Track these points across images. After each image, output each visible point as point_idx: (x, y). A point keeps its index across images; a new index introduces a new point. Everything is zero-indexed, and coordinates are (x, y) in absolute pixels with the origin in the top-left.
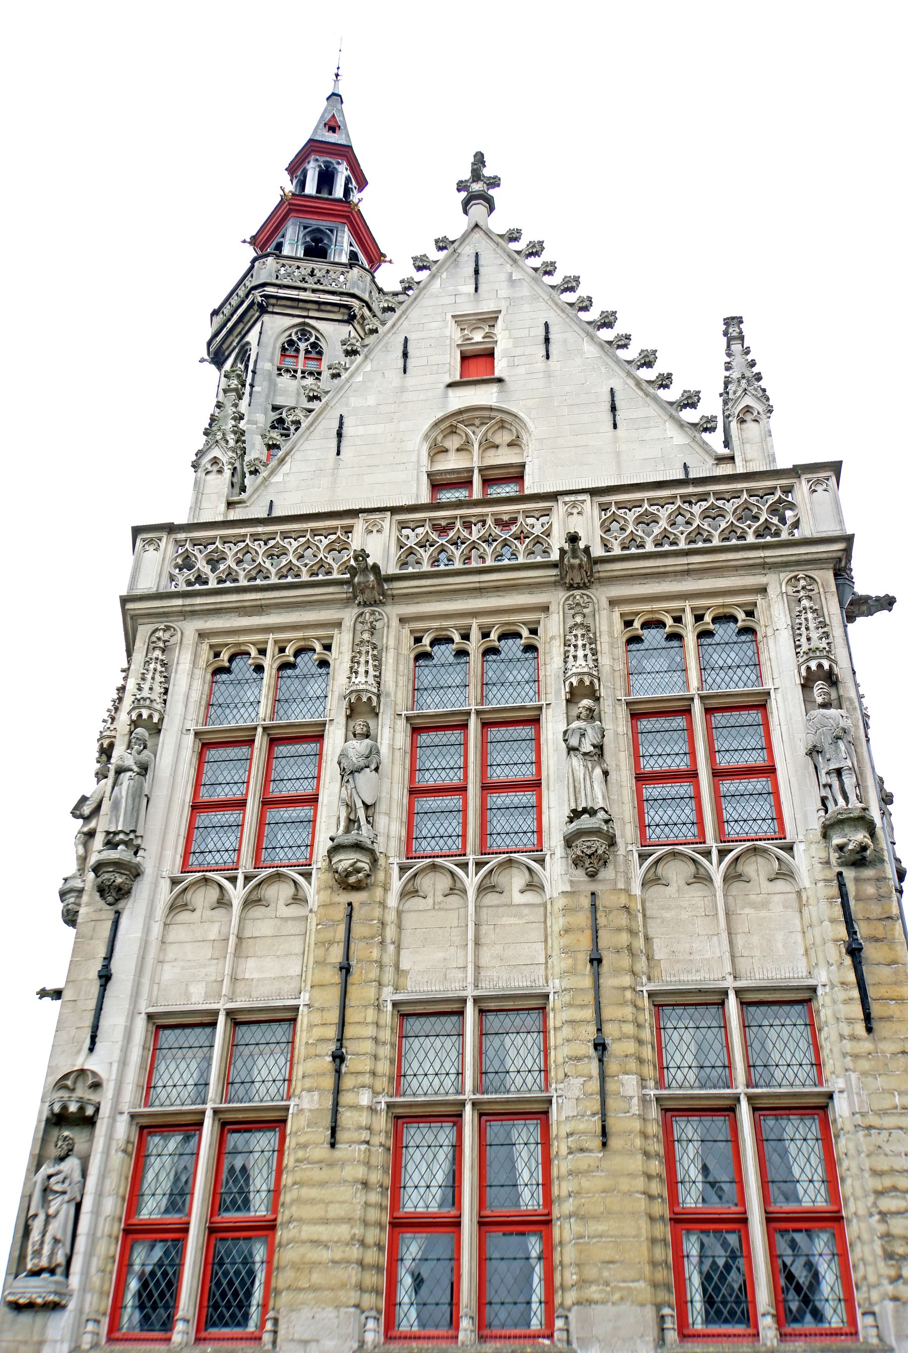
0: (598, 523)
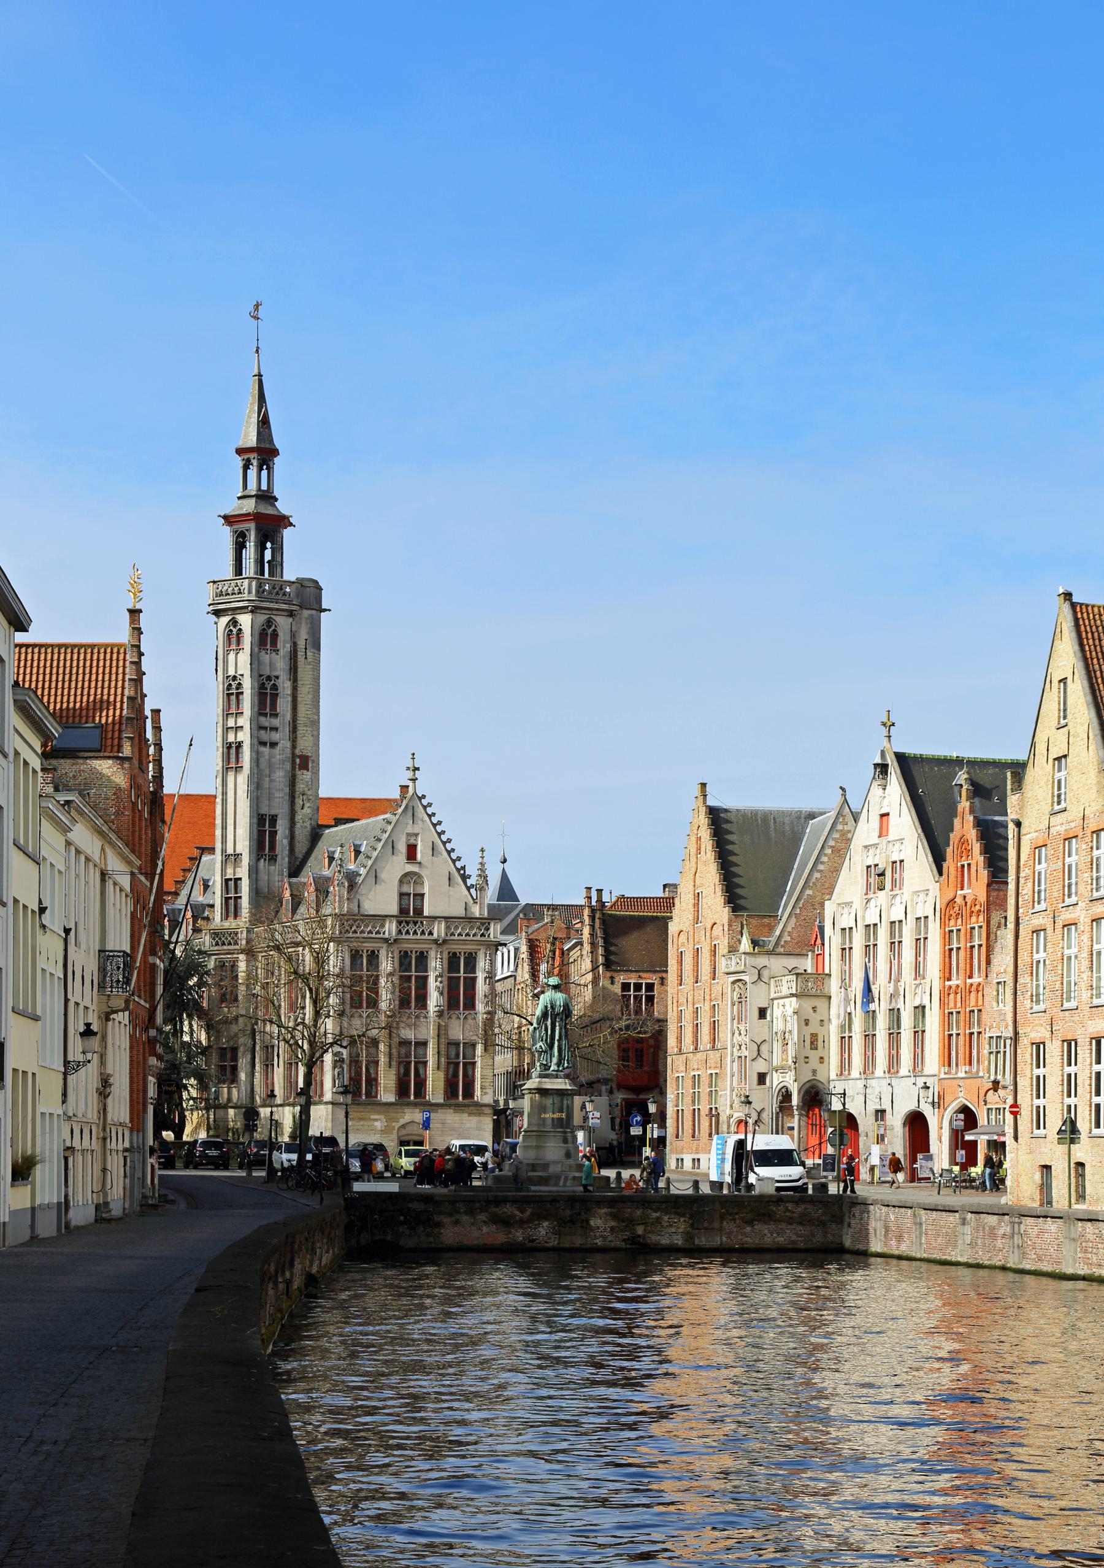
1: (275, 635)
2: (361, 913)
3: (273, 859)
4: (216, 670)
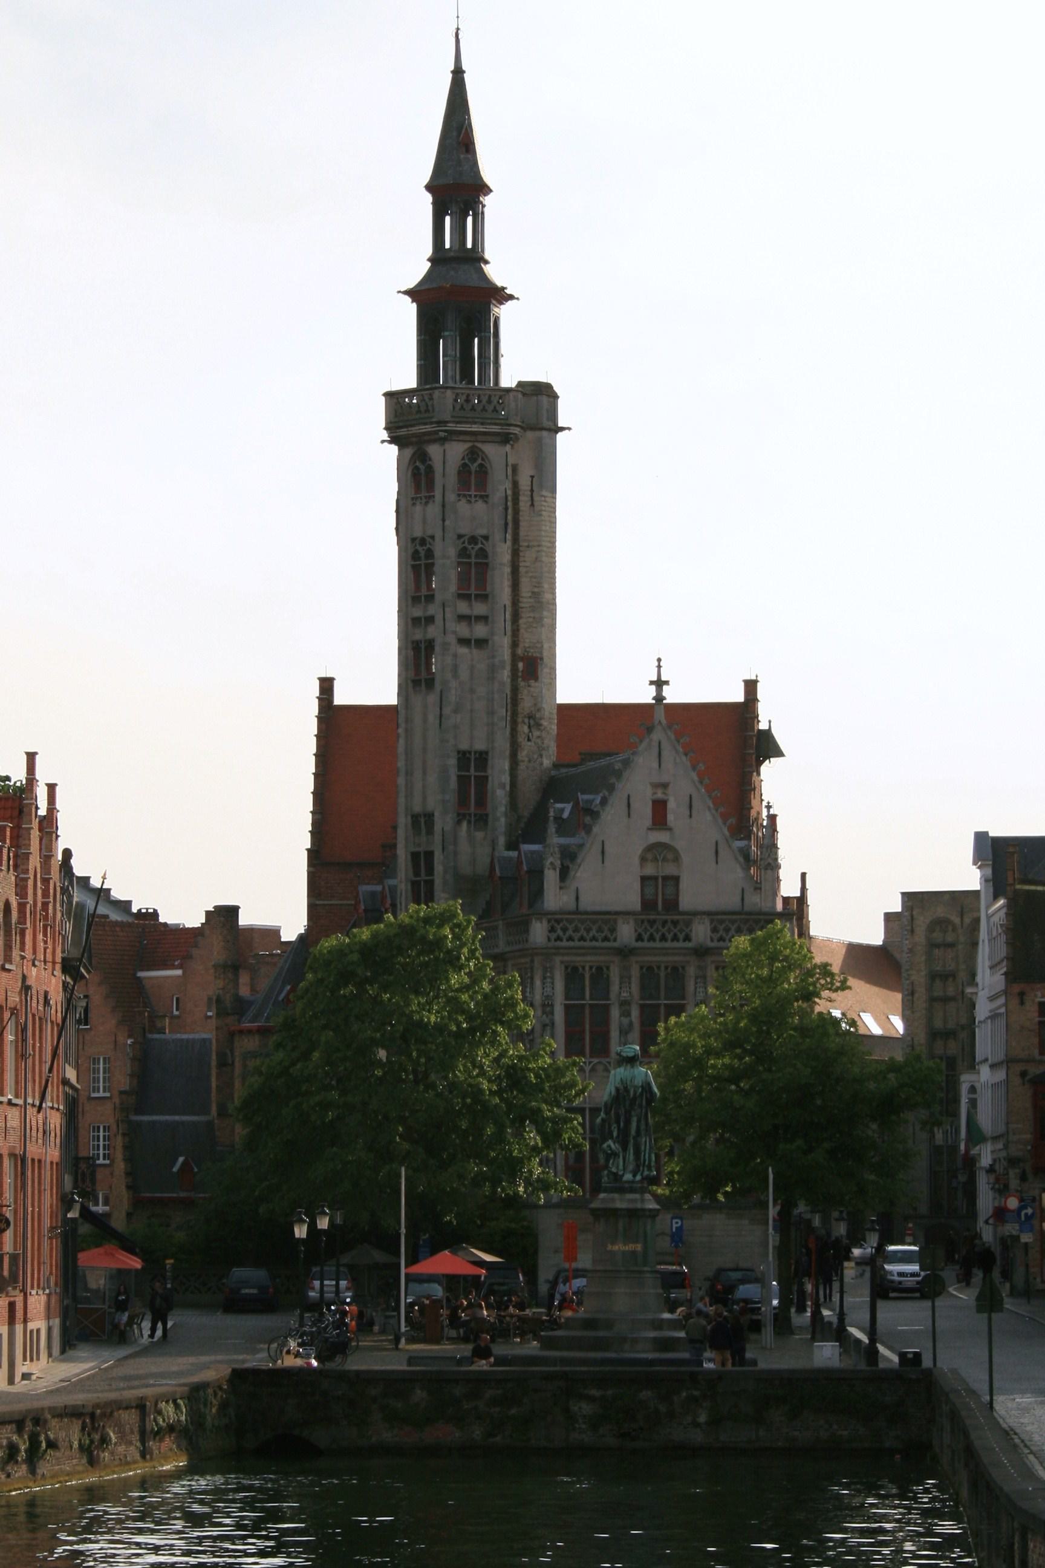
0: (709, 929)
1: (483, 473)
2: (582, 907)
3: (482, 820)
4: (397, 529)
